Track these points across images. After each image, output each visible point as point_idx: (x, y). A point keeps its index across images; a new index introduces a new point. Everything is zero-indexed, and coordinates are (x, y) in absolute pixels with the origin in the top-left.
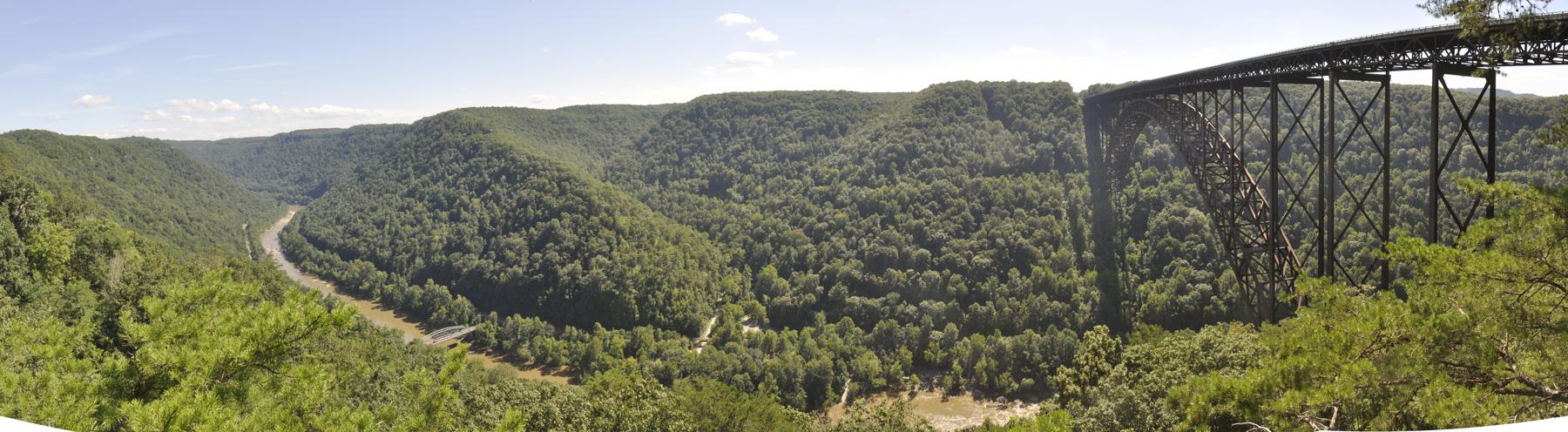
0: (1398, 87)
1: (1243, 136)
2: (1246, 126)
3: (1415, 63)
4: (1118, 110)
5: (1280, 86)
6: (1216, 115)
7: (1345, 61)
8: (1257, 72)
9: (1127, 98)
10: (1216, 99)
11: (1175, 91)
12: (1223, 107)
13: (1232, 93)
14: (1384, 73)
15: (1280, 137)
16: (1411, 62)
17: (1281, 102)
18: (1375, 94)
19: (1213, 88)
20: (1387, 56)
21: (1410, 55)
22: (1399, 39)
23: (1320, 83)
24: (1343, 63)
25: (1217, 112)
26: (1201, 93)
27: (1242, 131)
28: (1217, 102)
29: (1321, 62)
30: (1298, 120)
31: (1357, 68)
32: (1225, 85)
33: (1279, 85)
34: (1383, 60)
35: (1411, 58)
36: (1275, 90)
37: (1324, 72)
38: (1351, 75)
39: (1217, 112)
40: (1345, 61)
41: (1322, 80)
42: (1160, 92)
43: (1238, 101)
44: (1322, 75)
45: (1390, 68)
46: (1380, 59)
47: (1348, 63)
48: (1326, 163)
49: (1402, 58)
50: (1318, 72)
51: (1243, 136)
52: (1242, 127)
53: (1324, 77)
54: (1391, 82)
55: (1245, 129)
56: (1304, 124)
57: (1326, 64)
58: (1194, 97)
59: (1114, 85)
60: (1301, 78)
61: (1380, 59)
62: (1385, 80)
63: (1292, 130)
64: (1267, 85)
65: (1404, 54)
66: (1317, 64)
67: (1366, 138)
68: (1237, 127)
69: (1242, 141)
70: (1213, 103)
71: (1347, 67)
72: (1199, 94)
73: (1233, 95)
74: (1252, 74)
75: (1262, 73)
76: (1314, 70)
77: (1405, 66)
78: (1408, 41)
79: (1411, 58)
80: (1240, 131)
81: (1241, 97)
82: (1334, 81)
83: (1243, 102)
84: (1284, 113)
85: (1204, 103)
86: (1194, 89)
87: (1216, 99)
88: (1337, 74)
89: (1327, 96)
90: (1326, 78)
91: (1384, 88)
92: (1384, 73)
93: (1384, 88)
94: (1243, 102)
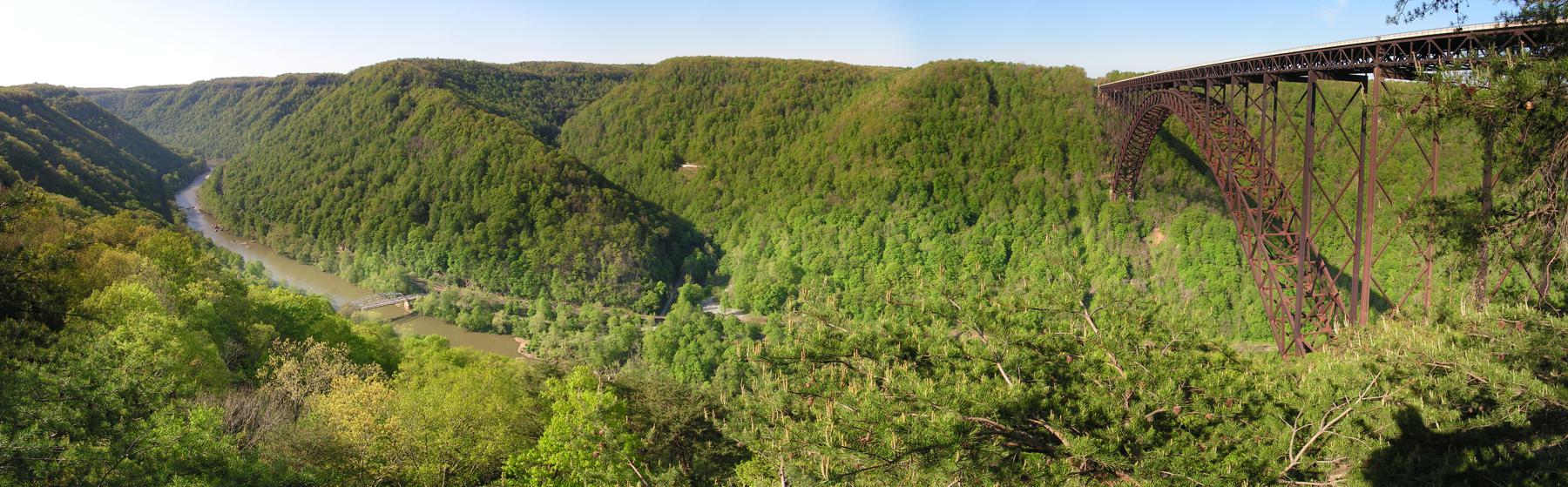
1: (1274, 135)
7: (1392, 58)
11: (1203, 83)
13: (1265, 87)
21: (1464, 53)
23: (1365, 80)
24: (1390, 60)
28: (1247, 97)
29: (1367, 57)
30: (1337, 120)
32: (1258, 79)
33: (1318, 81)
35: (1466, 56)
37: (1370, 70)
40: (1392, 58)
44: (1366, 72)
46: (1432, 57)
48: (1366, 171)
50: (1362, 70)
51: (1274, 135)
56: (1344, 125)
57: (1371, 60)
59: (1134, 74)
61: (1432, 57)
63: (1330, 131)
64: (1305, 80)
65: (1458, 53)
66: (1361, 60)
68: (1268, 124)
69: (1273, 143)
70: (1243, 94)
72: (1228, 86)
73: (1266, 90)
74: (1289, 68)
79: (1466, 56)
90: (1371, 76)
94: (1276, 100)
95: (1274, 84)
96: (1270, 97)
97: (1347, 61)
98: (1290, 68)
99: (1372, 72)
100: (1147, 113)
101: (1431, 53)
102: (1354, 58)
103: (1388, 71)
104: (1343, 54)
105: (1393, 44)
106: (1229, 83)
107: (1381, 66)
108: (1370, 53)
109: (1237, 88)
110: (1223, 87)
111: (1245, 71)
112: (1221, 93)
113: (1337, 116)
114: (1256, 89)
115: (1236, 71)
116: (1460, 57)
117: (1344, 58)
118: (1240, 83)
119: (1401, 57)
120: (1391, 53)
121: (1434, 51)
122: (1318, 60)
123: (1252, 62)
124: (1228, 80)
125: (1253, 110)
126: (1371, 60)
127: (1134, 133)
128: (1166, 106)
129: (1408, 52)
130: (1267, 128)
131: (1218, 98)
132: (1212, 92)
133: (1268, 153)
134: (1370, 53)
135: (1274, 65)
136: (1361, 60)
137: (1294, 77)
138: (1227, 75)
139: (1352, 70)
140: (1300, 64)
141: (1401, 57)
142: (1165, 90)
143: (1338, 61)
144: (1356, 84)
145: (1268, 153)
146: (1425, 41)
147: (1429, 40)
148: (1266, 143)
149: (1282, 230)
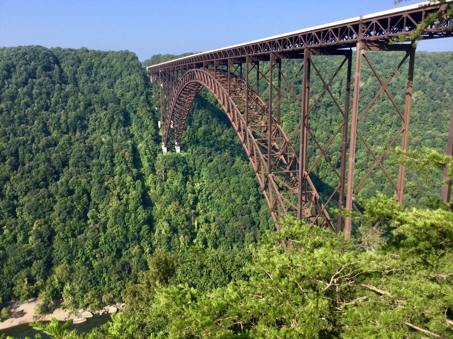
0: (423, 55)
11: (225, 62)
13: (272, 63)
18: (400, 61)
23: (349, 55)
28: (258, 72)
29: (351, 35)
30: (326, 87)
32: (266, 58)
37: (354, 44)
40: (372, 33)
41: (351, 51)
47: (376, 35)
53: (352, 48)
58: (240, 67)
59: (173, 57)
61: (407, 29)
66: (346, 37)
72: (244, 65)
73: (273, 66)
75: (297, 46)
85: (248, 73)
90: (354, 49)
91: (409, 57)
93: (409, 57)
95: (279, 61)
100: (185, 87)
101: (406, 26)
102: (341, 36)
103: (369, 45)
104: (332, 33)
105: (374, 21)
106: (245, 62)
107: (364, 41)
108: (354, 31)
109: (250, 66)
110: (240, 65)
111: (256, 52)
114: (265, 66)
117: (332, 36)
118: (252, 62)
119: (381, 32)
121: (409, 23)
123: (261, 45)
124: (244, 60)
127: (177, 103)
128: (199, 81)
129: (385, 27)
131: (236, 73)
132: (232, 69)
134: (354, 31)
135: (278, 46)
136: (346, 37)
138: (243, 56)
139: (340, 46)
140: (298, 44)
141: (381, 32)
142: (197, 69)
143: (327, 39)
144: (344, 57)
146: (402, 16)
149: (286, 169)
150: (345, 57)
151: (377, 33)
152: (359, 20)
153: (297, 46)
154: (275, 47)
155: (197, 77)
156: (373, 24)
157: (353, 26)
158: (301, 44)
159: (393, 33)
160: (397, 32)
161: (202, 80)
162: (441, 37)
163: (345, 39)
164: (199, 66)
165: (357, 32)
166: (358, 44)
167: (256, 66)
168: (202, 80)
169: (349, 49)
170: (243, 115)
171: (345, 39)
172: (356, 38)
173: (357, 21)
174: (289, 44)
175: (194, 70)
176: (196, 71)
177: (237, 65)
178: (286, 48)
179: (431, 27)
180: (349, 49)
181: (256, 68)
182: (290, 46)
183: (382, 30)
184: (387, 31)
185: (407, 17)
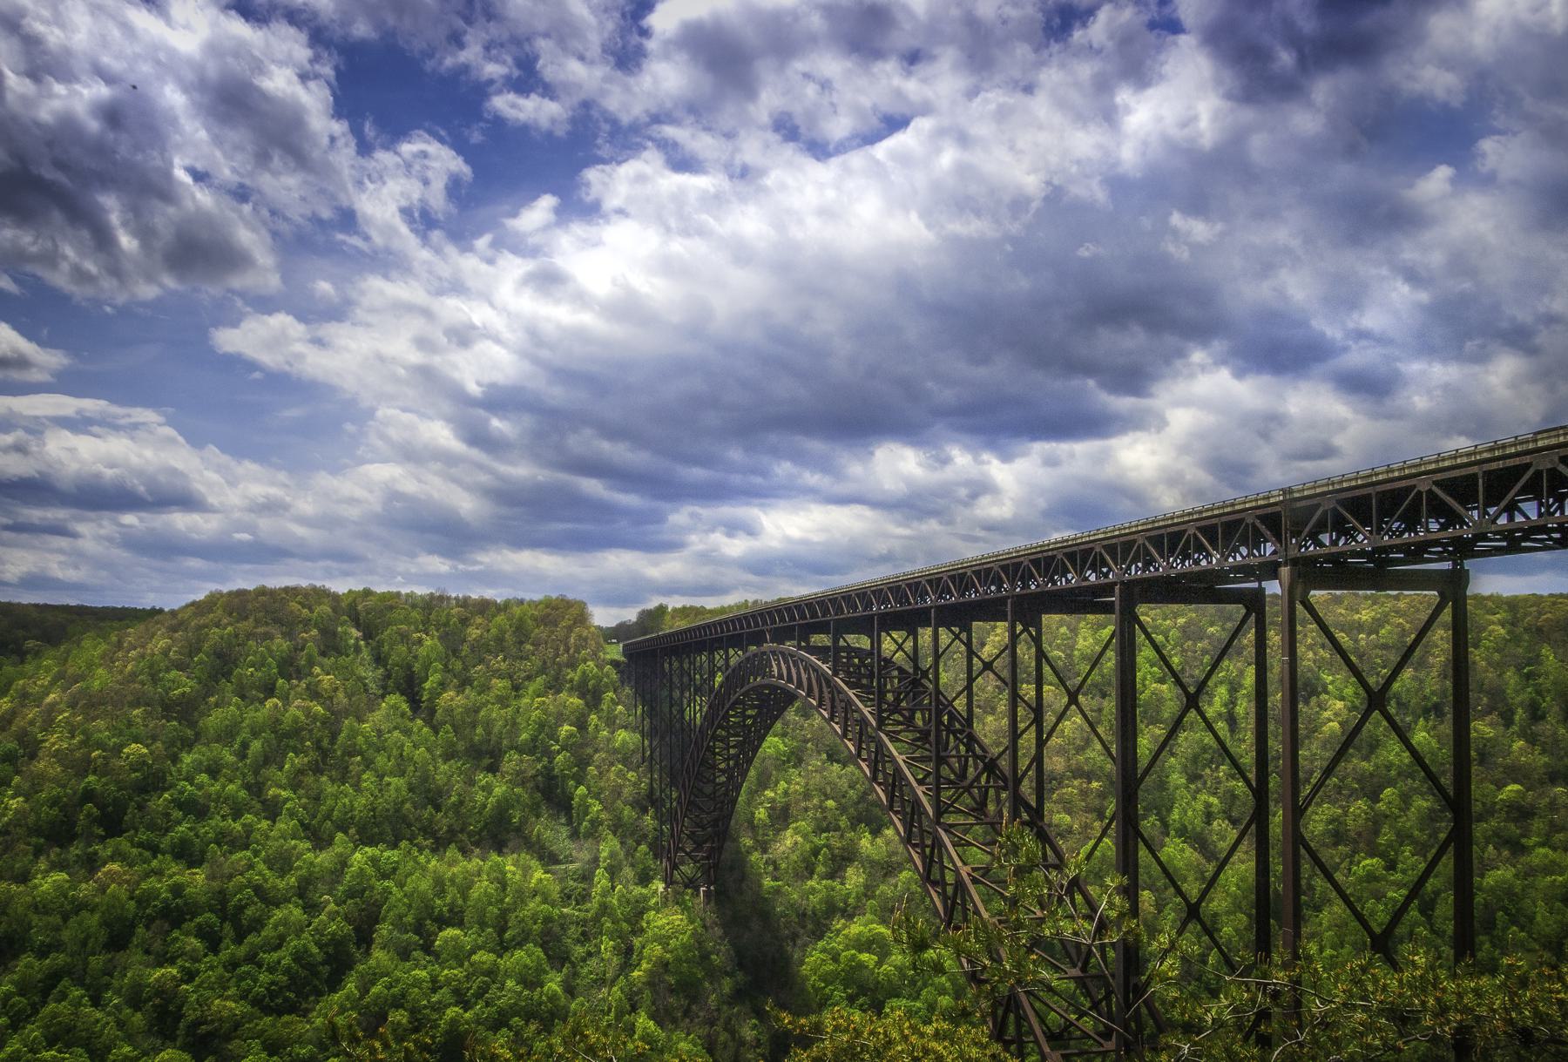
1: (1041, 743)
2: (1049, 718)
3: (1548, 531)
4: (713, 675)
5: (1141, 609)
6: (969, 688)
7: (1325, 538)
8: (1080, 573)
9: (737, 641)
10: (968, 644)
11: (863, 625)
12: (988, 666)
14: (1446, 565)
15: (1145, 743)
16: (1530, 531)
17: (1145, 654)
19: (960, 617)
20: (1453, 519)
21: (1531, 509)
22: (1494, 466)
23: (1255, 603)
24: (1322, 545)
25: (971, 680)
26: (929, 631)
27: (1039, 732)
28: (971, 653)
31: (1362, 554)
32: (991, 610)
33: (1141, 609)
34: (1444, 527)
35: (1534, 517)
36: (1128, 622)
37: (1271, 570)
38: (1340, 573)
39: (971, 680)
40: (1325, 538)
41: (1261, 591)
42: (822, 628)
43: (1026, 653)
44: (1260, 580)
45: (1463, 549)
46: (1434, 526)
47: (1334, 543)
49: (1503, 521)
51: (1041, 743)
52: (1038, 720)
54: (1471, 591)
55: (1047, 726)
56: (1210, 712)
57: (1270, 548)
60: (1201, 589)
61: (1434, 526)
62: (1453, 587)
63: (1177, 726)
64: (1107, 609)
65: (1511, 509)
66: (1244, 551)
67: (1393, 752)
69: (1038, 759)
71: (1337, 560)
72: (925, 635)
73: (1014, 638)
75: (1093, 578)
76: (1236, 569)
77: (1514, 543)
78: (1528, 466)
79: (1534, 517)
80: (1033, 728)
81: (1037, 640)
82: (1296, 596)
83: (1041, 655)
84: (1153, 687)
85: (937, 657)
86: (910, 621)
87: (968, 644)
88: (1310, 573)
89: (1274, 638)
90: (1273, 588)
92: (1446, 565)
94: (1041, 655)
96: (1026, 653)
97: (1209, 555)
98: (1068, 581)
99: (1274, 575)
105: (1328, 505)
111: (963, 595)
112: (909, 645)
113: (1192, 690)
114: (993, 637)
115: (940, 597)
116: (1519, 519)
120: (1321, 527)
121: (1438, 509)
122: (1135, 561)
123: (977, 573)
125: (987, 685)
126: (1270, 548)
130: (1022, 726)
133: (1027, 788)
137: (1080, 602)
139: (1220, 575)
141: (1349, 533)
144: (1238, 610)
145: (1027, 788)
147: (1424, 486)
148: (1023, 763)
150: (1243, 611)
151: (1338, 539)
152: (1281, 502)
153: (1093, 578)
154: (1022, 579)
155: (775, 668)
156: (1325, 512)
157: (1263, 518)
158: (1105, 570)
159: (1391, 537)
160: (1402, 533)
161: (790, 680)
162: (1546, 548)
163: (1239, 558)
164: (781, 635)
165: (1278, 537)
166: (1285, 571)
167: (964, 636)
168: (790, 680)
169: (1255, 585)
170: (923, 788)
171: (1239, 558)
172: (1275, 552)
173: (1275, 504)
174: (1064, 573)
175: (768, 646)
176: (774, 653)
177: (904, 634)
178: (1054, 583)
179: (1511, 519)
180: (1255, 585)
181: (961, 641)
182: (1070, 576)
183: (1354, 529)
184: (1371, 532)
185: (1430, 492)
